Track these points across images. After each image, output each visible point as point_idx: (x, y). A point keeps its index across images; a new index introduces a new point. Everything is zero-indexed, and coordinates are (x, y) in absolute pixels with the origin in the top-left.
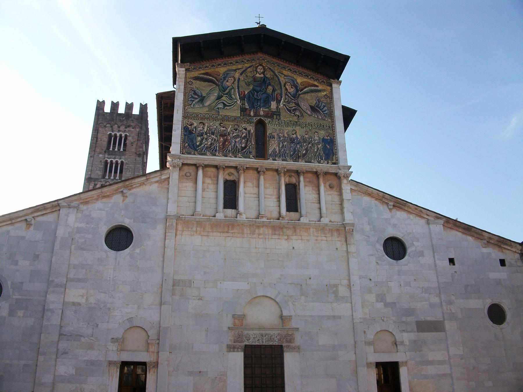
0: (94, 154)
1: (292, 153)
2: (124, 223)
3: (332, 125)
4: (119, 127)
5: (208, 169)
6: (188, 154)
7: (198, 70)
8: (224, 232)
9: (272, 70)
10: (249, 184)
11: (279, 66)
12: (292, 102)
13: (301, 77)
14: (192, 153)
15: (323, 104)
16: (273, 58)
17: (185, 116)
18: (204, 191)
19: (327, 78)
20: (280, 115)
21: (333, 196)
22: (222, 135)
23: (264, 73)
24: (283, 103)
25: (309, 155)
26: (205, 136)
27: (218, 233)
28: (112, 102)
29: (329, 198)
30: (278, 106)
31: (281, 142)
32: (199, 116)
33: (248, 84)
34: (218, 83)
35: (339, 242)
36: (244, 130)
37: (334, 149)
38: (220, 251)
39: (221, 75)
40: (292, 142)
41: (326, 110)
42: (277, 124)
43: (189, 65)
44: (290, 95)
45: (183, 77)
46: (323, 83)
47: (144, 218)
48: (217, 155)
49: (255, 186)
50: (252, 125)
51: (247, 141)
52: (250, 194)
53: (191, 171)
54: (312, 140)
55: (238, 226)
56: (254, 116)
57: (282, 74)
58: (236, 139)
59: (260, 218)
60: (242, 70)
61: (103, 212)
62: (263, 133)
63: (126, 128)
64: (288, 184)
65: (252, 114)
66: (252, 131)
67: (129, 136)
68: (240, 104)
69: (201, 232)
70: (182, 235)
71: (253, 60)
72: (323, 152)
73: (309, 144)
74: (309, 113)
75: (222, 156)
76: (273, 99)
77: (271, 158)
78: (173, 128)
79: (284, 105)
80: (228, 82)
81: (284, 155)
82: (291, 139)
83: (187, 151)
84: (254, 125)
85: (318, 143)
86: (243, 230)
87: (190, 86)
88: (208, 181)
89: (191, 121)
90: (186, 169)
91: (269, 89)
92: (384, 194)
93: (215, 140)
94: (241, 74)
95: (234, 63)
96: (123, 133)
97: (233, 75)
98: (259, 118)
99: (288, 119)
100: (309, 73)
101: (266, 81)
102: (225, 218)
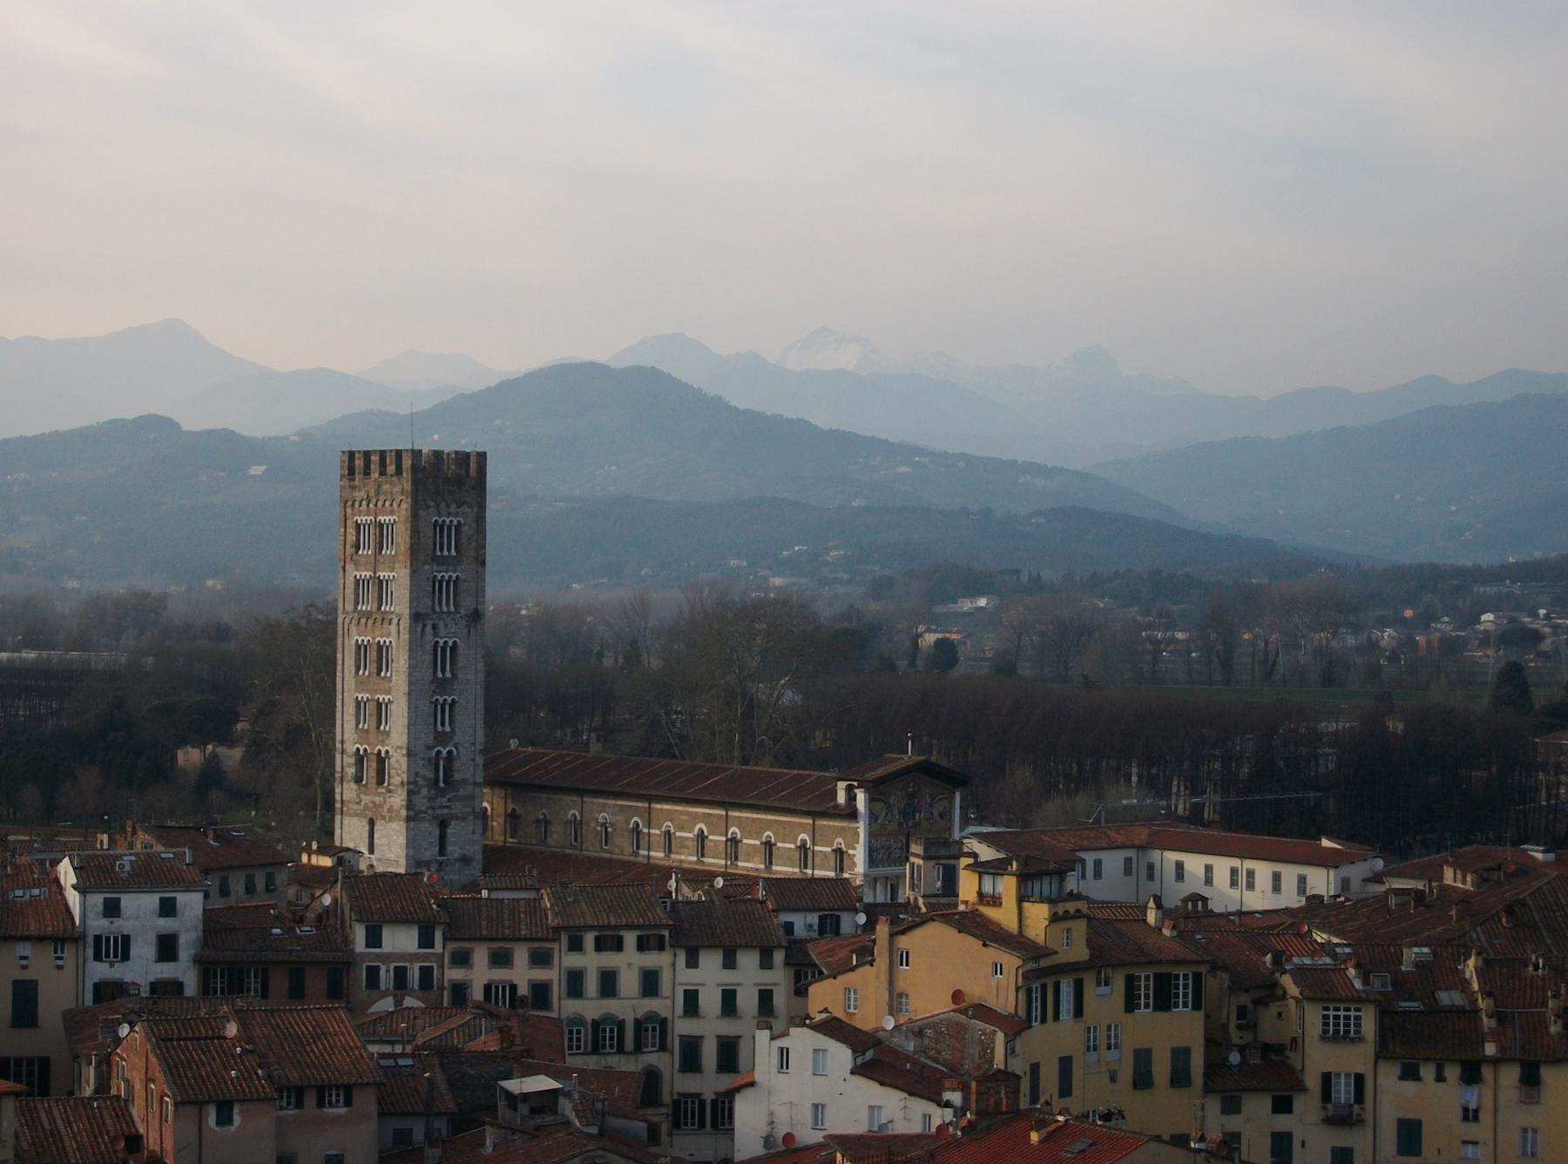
4: (448, 506)
63: (458, 507)
65: (905, 826)
96: (456, 518)
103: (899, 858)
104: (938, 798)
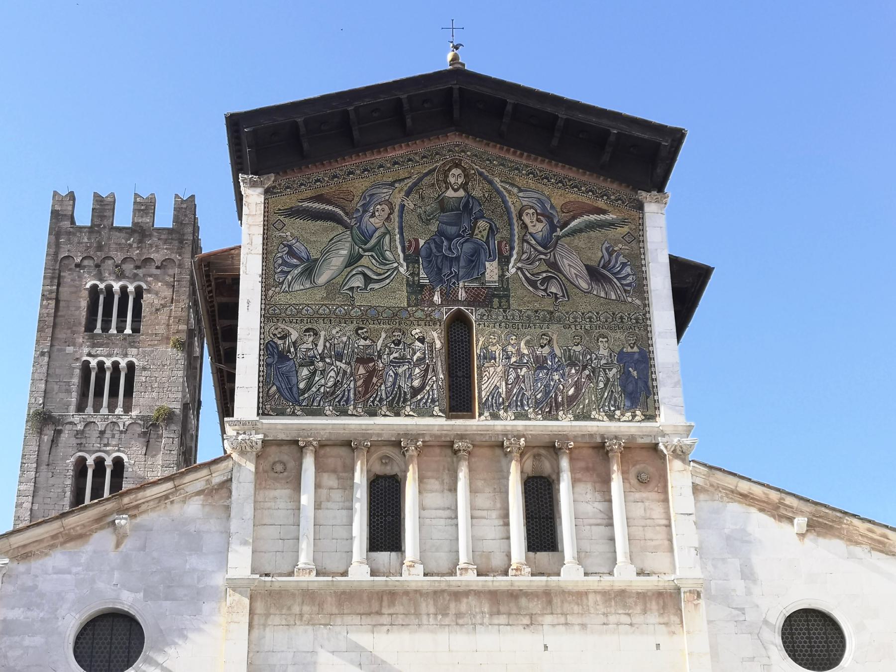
0: (52, 346)
1: (538, 397)
2: (121, 603)
3: (644, 315)
5: (328, 449)
6: (277, 415)
7: (296, 189)
8: (369, 614)
9: (485, 178)
10: (433, 484)
11: (503, 165)
12: (541, 259)
13: (560, 192)
14: (289, 410)
15: (622, 259)
16: (488, 145)
17: (269, 315)
18: (318, 509)
19: (631, 190)
20: (507, 297)
21: (647, 504)
22: (362, 361)
23: (465, 187)
24: (515, 264)
25: (584, 400)
26: (321, 364)
27: (354, 616)
28: (96, 195)
29: (638, 510)
30: (503, 272)
31: (511, 369)
32: (304, 312)
33: (427, 222)
34: (349, 221)
35: (663, 627)
36: (418, 343)
37: (650, 379)
38: (360, 664)
39: (356, 199)
40: (541, 367)
41: (629, 275)
42: (501, 322)
43: (273, 179)
44: (533, 242)
45: (259, 212)
46: (620, 202)
47: (169, 587)
48: (350, 412)
49: (446, 487)
50: (438, 326)
51: (426, 371)
52: (436, 509)
53: (285, 458)
54: (591, 359)
55: (404, 597)
56: (442, 305)
57: (513, 185)
58: (399, 367)
59: (458, 572)
60: (410, 182)
61: (68, 577)
62: (466, 345)
63: (137, 267)
64: (533, 477)
66: (438, 344)
67: (149, 291)
68: (408, 273)
69: (313, 616)
70: (265, 626)
71: (437, 154)
72: (620, 389)
73: (584, 369)
74: (584, 285)
75: (362, 413)
76: (490, 256)
77: (487, 414)
78: (239, 351)
79: (518, 268)
80: (375, 216)
81: (519, 404)
82: (537, 359)
83: (274, 407)
84: (443, 327)
85: (609, 366)
86: (416, 606)
87: (278, 234)
88: (330, 480)
89: (283, 326)
90: (274, 453)
91: (479, 228)
92: (783, 495)
93: (345, 372)
94: (408, 194)
95: (389, 165)
96: (131, 283)
97: (387, 198)
98: (456, 308)
99: (531, 306)
100: (585, 178)
101: (473, 205)
102: (372, 575)
103: (416, 391)
104: (573, 224)
